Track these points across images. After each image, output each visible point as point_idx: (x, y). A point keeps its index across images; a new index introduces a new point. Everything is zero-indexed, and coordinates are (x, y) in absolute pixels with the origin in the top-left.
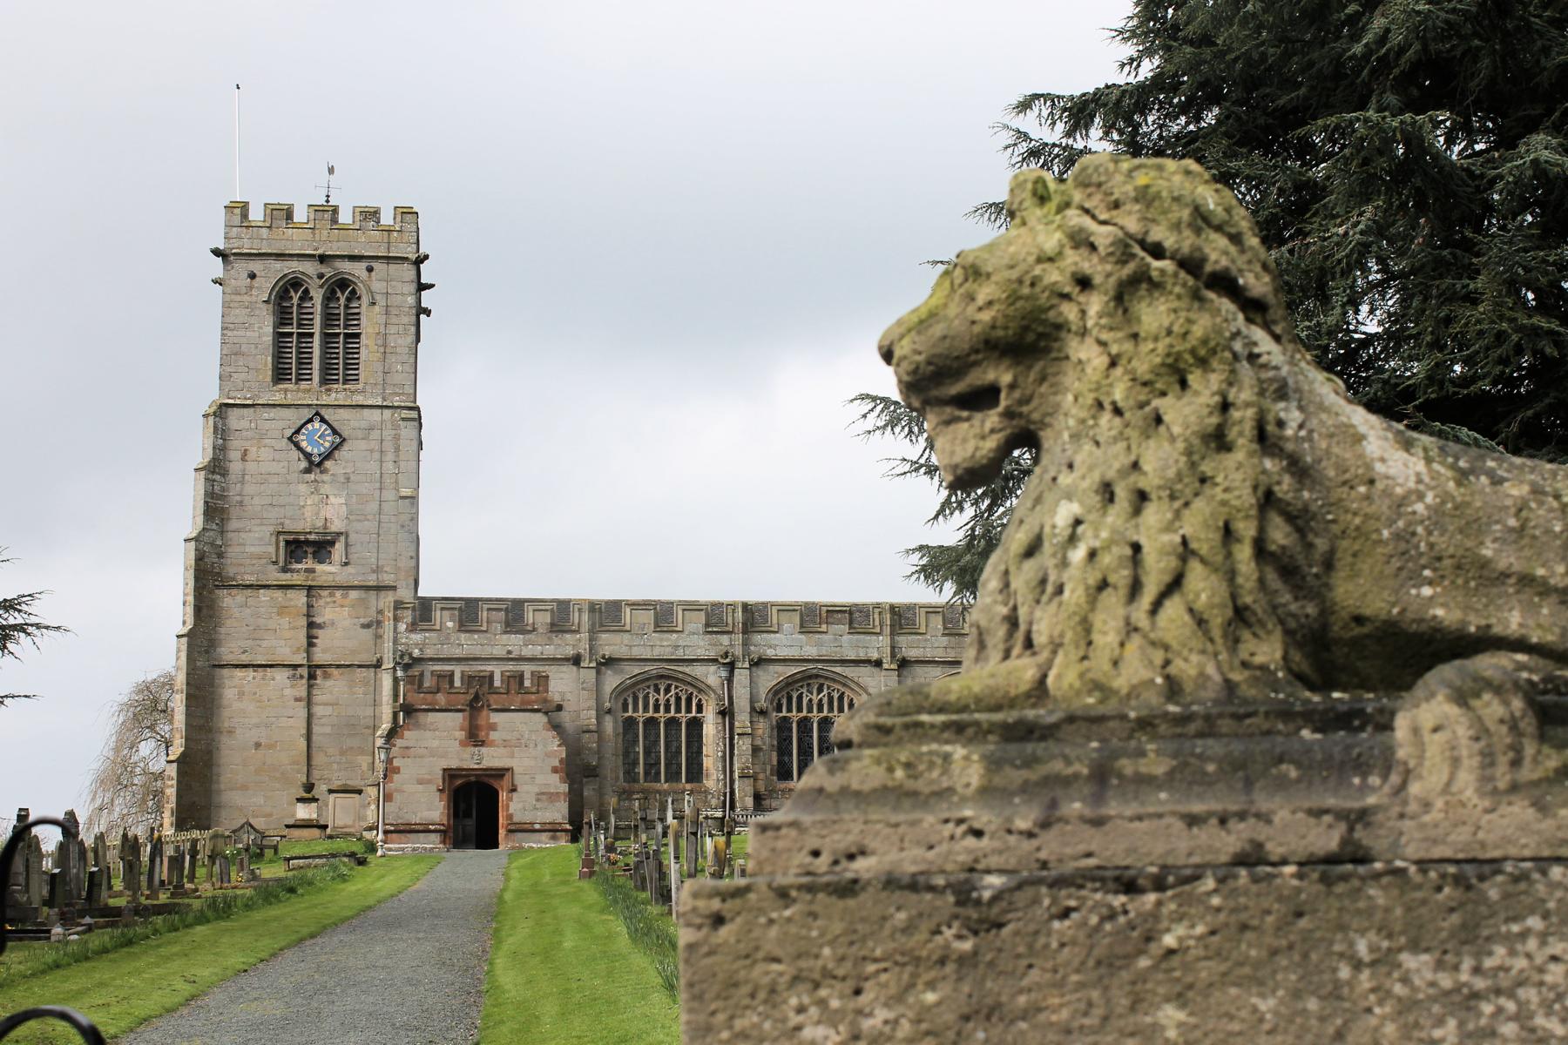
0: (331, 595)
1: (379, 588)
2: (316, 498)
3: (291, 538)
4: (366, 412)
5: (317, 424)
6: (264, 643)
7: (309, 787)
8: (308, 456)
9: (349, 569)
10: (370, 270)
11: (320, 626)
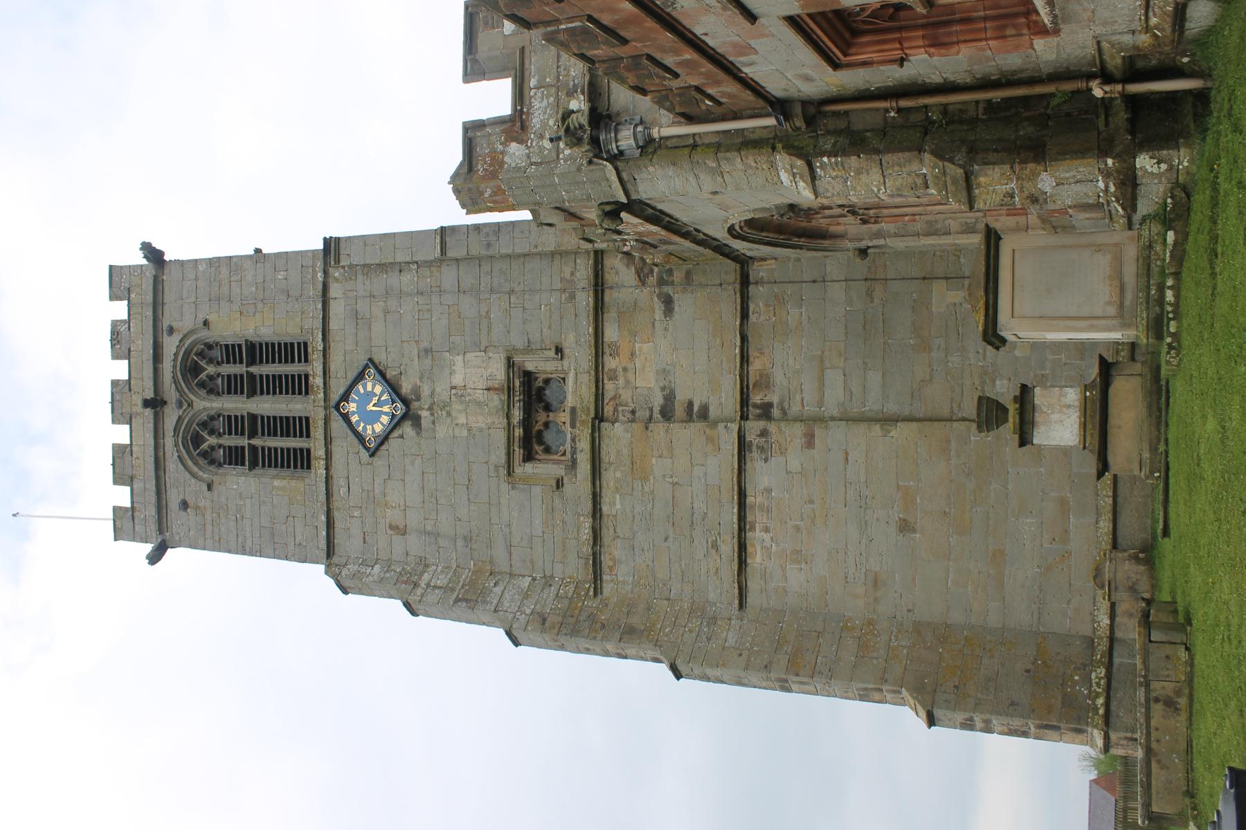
0: (613, 378)
1: (599, 286)
2: (457, 406)
3: (518, 453)
4: (334, 325)
5: (352, 407)
6: (700, 506)
7: (990, 414)
8: (396, 423)
9: (569, 343)
10: (171, 331)
11: (670, 398)
